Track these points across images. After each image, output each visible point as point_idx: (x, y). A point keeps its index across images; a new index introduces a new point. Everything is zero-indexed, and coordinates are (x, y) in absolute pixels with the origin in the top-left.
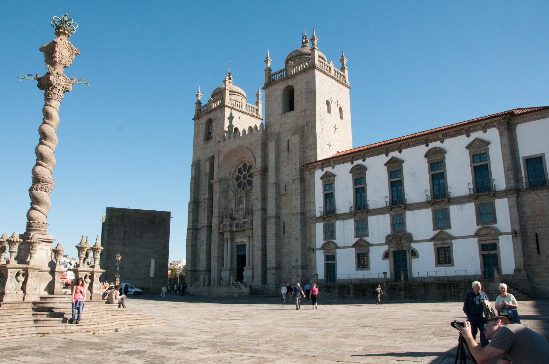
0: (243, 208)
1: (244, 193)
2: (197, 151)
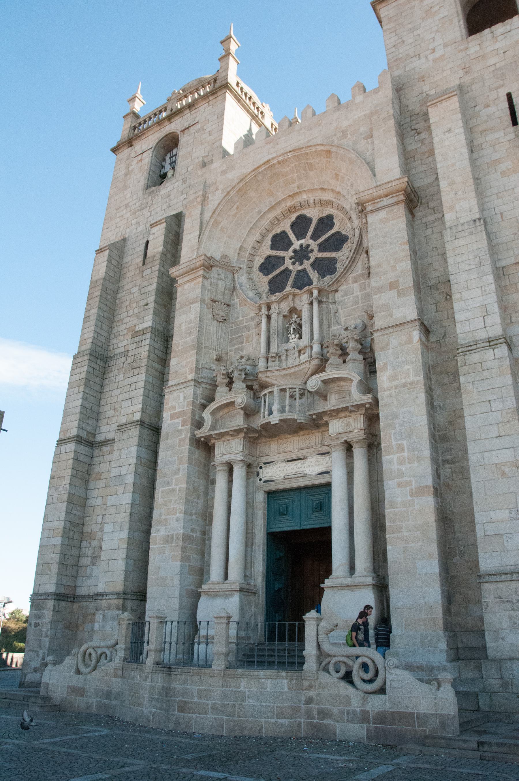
0: (305, 341)
2: (118, 220)
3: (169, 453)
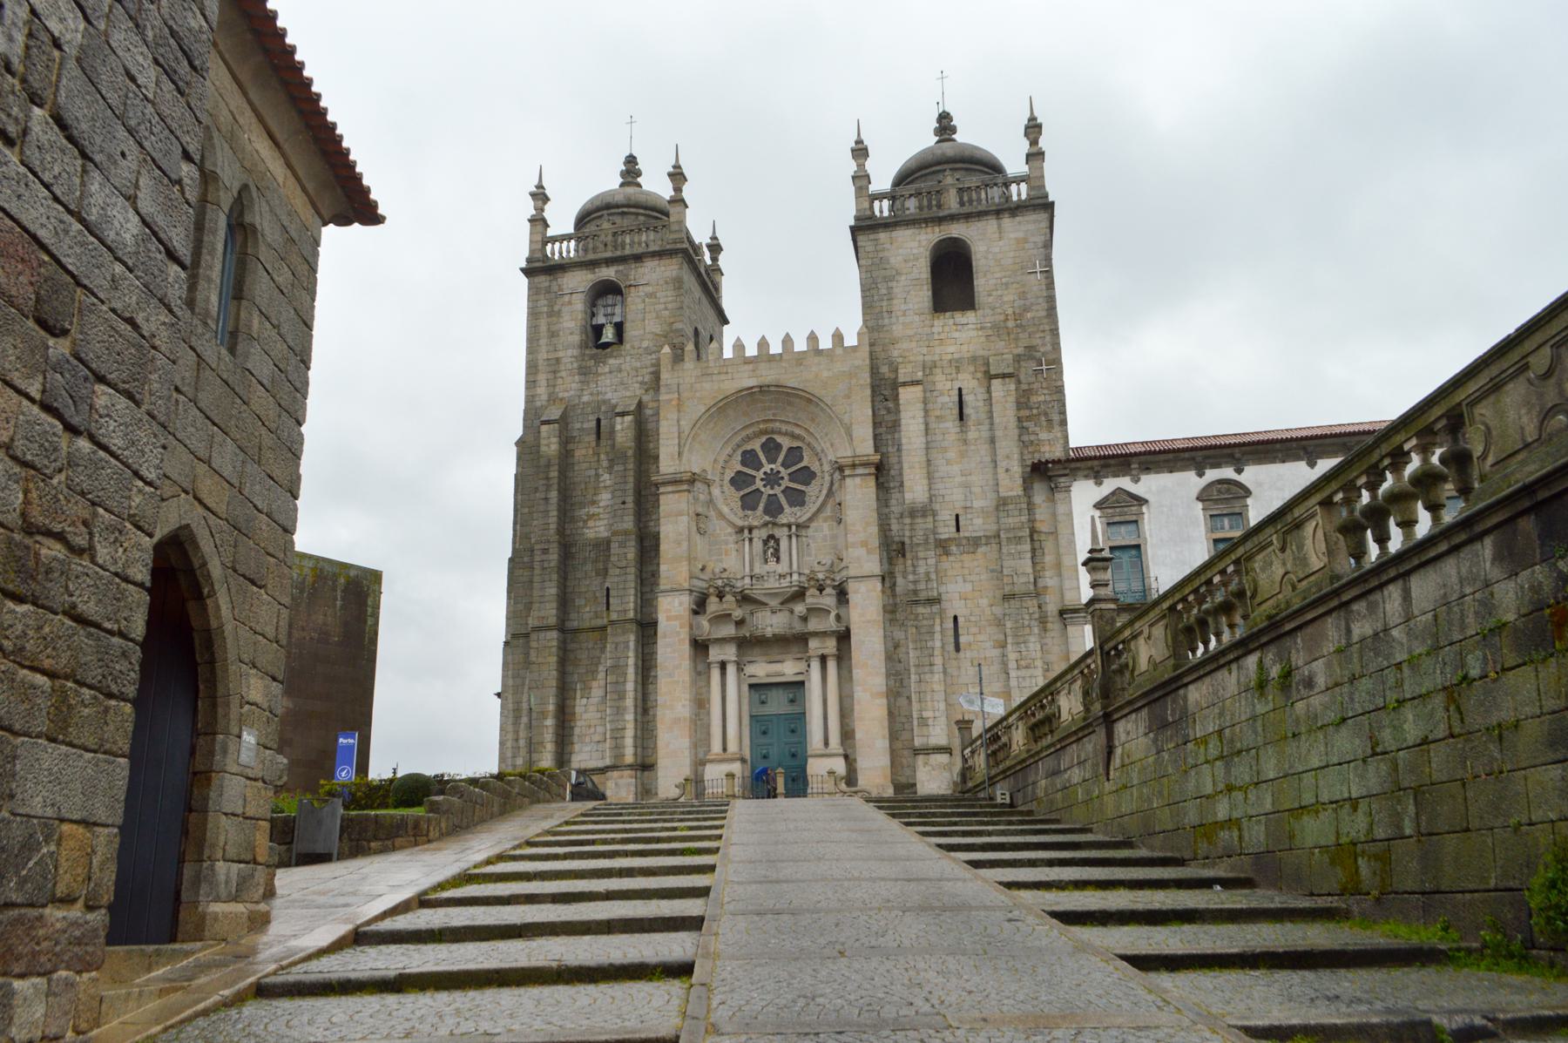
1: (789, 526)
3: (669, 650)
